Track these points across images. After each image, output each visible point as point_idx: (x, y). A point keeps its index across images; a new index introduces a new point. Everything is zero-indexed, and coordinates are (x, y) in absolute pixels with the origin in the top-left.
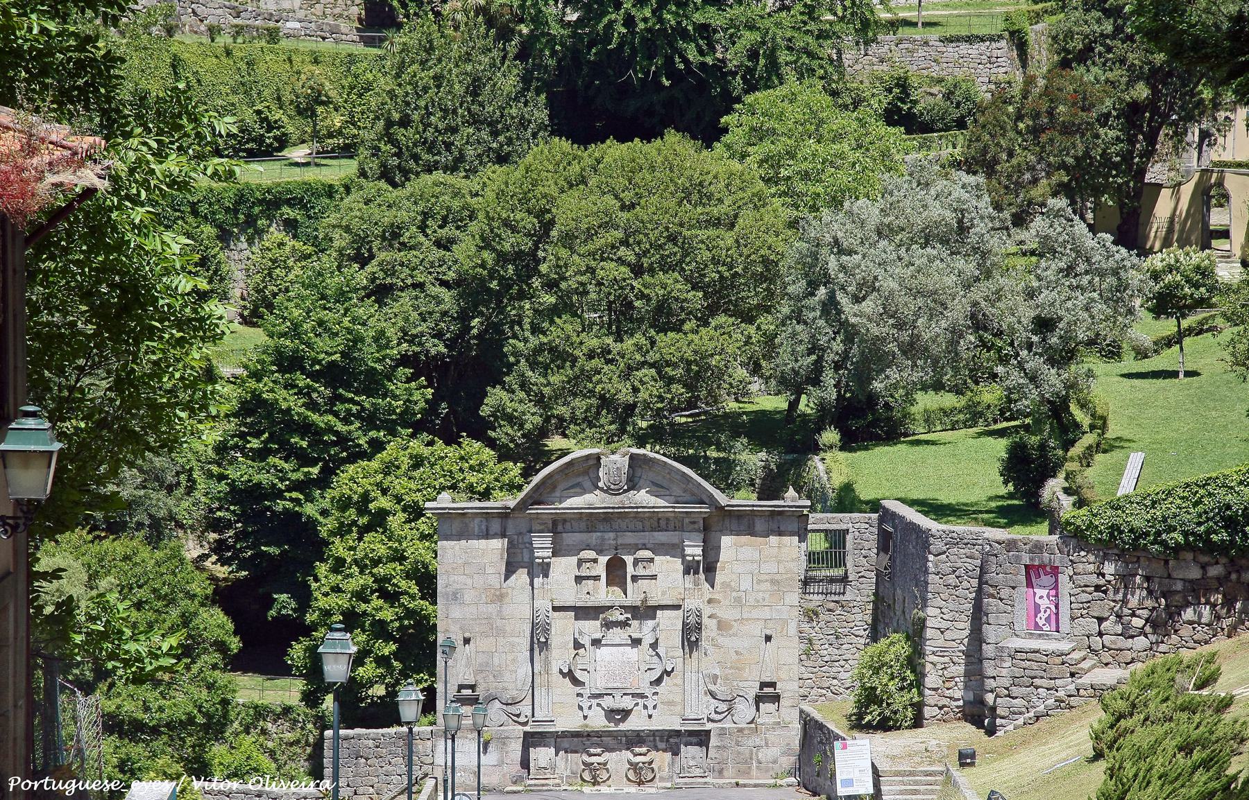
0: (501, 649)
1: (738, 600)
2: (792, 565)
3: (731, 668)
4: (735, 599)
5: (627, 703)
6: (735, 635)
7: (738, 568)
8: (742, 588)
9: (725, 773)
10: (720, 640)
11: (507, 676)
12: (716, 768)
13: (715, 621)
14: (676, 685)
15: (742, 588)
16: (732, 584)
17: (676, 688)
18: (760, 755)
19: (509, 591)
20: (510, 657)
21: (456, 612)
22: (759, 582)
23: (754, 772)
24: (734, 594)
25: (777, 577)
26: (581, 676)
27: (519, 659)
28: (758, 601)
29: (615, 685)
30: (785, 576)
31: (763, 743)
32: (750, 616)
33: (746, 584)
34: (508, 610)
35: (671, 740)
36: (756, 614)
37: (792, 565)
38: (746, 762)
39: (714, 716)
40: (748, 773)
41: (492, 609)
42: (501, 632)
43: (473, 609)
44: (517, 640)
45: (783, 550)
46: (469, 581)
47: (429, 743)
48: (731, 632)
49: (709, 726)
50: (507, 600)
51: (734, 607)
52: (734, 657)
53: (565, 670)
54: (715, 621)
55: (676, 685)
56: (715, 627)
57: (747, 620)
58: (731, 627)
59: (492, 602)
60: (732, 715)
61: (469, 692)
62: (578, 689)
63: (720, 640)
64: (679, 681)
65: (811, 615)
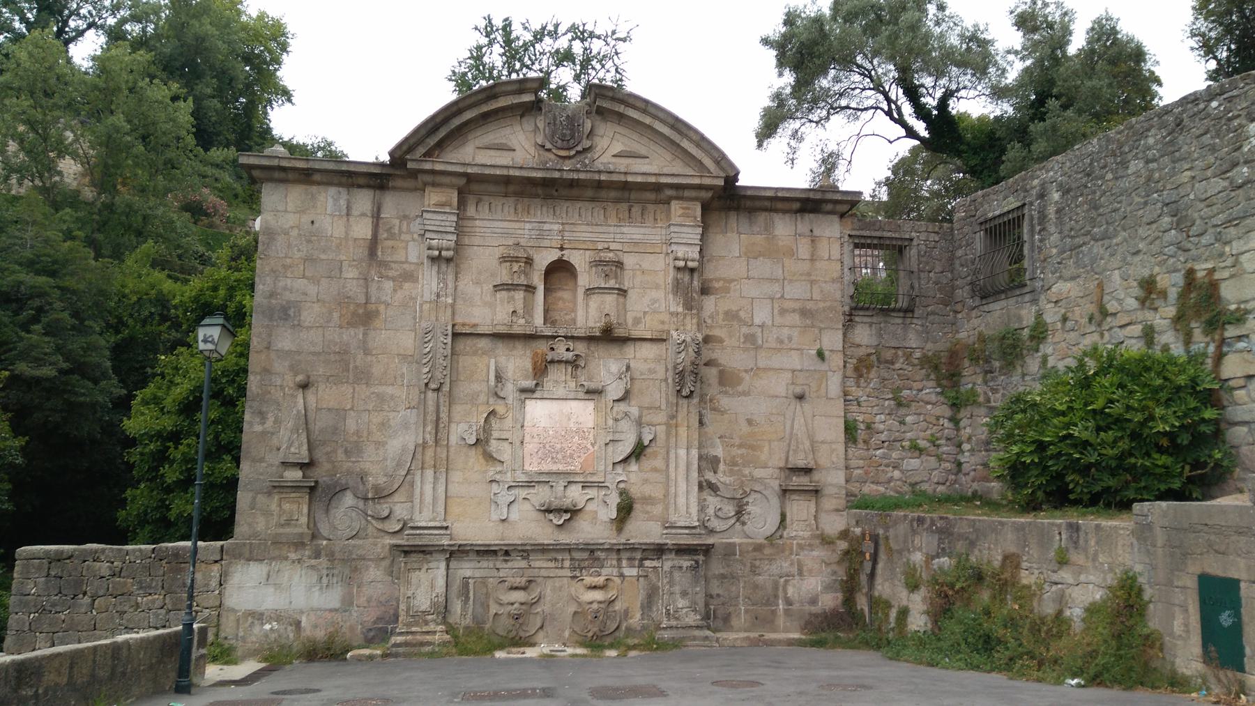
1: (750, 338)
2: (829, 288)
3: (740, 446)
5: (575, 495)
6: (746, 394)
7: (751, 290)
8: (757, 321)
9: (735, 622)
10: (724, 402)
11: (370, 453)
14: (655, 470)
15: (757, 321)
16: (742, 314)
17: (656, 475)
18: (790, 591)
19: (382, 308)
21: (285, 340)
22: (783, 312)
23: (781, 621)
24: (745, 330)
25: (810, 305)
26: (498, 451)
27: (392, 423)
28: (782, 342)
29: (554, 468)
30: (821, 305)
31: (795, 570)
33: (762, 315)
34: (380, 337)
35: (647, 563)
36: (777, 361)
37: (829, 288)
38: (768, 603)
40: (772, 622)
41: (352, 336)
42: (363, 376)
44: (389, 390)
45: (818, 264)
46: (312, 290)
47: (216, 567)
48: (740, 388)
50: (377, 323)
52: (745, 428)
55: (655, 470)
57: (766, 369)
58: (739, 381)
59: (351, 324)
60: (744, 524)
61: (297, 474)
62: (492, 472)
63: (724, 402)
65: (861, 368)
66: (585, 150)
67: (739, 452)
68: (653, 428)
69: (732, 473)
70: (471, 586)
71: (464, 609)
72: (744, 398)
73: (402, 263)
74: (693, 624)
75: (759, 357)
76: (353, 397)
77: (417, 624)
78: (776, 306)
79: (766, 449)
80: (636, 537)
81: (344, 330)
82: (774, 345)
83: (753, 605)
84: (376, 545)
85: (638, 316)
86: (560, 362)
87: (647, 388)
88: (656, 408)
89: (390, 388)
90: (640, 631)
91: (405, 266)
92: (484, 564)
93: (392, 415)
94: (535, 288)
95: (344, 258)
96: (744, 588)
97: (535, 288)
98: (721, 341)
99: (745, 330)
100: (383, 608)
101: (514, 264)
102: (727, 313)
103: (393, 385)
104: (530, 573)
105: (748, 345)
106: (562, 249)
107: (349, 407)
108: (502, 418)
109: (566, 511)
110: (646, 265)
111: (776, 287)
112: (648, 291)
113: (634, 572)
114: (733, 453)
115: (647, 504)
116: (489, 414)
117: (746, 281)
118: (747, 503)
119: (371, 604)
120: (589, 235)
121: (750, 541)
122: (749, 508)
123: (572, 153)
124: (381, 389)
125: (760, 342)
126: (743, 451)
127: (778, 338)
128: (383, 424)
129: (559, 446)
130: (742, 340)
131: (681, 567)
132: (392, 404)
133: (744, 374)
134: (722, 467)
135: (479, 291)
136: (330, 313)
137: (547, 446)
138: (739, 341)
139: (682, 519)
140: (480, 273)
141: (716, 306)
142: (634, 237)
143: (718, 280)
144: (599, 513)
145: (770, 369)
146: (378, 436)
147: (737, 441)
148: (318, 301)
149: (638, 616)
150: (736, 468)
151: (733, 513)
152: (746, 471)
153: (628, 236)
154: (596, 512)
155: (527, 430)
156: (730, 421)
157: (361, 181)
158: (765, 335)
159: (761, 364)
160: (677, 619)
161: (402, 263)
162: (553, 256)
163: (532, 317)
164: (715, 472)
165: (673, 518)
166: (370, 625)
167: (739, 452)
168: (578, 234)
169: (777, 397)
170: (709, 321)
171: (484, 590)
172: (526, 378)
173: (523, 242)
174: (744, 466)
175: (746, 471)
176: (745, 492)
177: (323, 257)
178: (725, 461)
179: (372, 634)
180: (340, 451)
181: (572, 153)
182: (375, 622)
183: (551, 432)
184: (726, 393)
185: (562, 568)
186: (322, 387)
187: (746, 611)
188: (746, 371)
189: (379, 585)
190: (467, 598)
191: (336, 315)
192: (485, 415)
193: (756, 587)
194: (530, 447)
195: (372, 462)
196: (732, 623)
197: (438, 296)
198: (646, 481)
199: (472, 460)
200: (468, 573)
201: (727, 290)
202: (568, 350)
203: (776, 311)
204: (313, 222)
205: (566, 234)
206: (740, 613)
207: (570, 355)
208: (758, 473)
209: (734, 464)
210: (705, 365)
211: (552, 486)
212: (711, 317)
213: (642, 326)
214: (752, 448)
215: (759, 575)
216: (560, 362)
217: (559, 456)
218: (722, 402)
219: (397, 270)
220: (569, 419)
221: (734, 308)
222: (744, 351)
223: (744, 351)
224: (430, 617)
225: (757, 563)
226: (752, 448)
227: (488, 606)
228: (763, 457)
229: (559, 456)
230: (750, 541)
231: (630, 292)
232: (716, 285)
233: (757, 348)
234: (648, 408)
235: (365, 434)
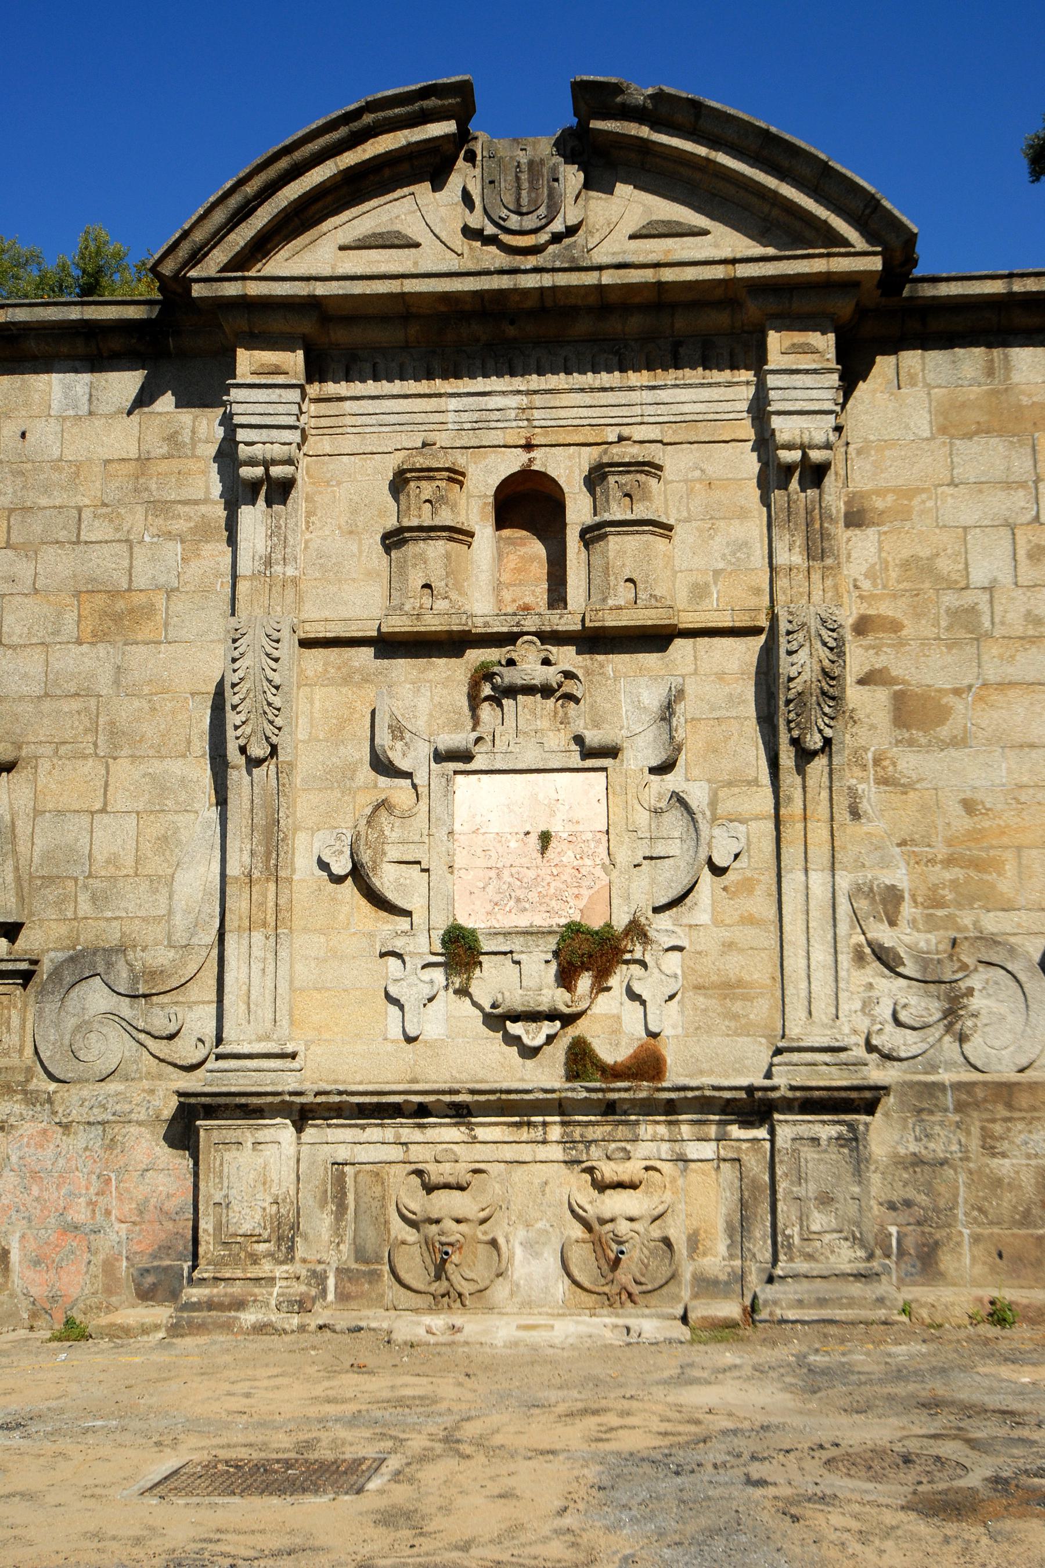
0: (119, 801)
3: (949, 862)
4: (954, 614)
6: (959, 742)
8: (979, 576)
9: (946, 1261)
12: (910, 1244)
13: (882, 695)
14: (749, 920)
15: (979, 576)
16: (944, 565)
17: (751, 932)
19: (160, 600)
20: (154, 828)
24: (950, 599)
26: (400, 887)
27: (184, 835)
32: (1013, 672)
39: (890, 1038)
43: (32, 663)
46: (24, 569)
48: (944, 732)
49: (877, 1074)
51: (953, 644)
52: (962, 822)
53: (341, 866)
54: (882, 695)
55: (749, 920)
56: (883, 718)
57: (1004, 686)
58: (943, 714)
59: (98, 637)
60: (962, 1038)
64: (763, 906)
66: (572, 231)
67: (948, 875)
68: (742, 828)
69: (931, 924)
70: (349, 1182)
71: (337, 1230)
72: (953, 752)
73: (196, 502)
74: (848, 1268)
75: (985, 658)
76: (106, 785)
77: (236, 1261)
78: (1021, 540)
79: (1010, 869)
80: (711, 1072)
81: (85, 648)
82: (1019, 631)
83: (991, 1223)
84: (152, 1092)
85: (701, 579)
86: (529, 690)
87: (727, 739)
88: (749, 783)
89: (180, 762)
90: (727, 1283)
91: (203, 509)
92: (374, 1133)
93: (182, 819)
94: (471, 535)
95: (87, 502)
96: (968, 1186)
97: (471, 535)
98: (895, 627)
99: (950, 599)
100: (169, 1225)
101: (424, 484)
102: (906, 565)
103: (184, 756)
104: (480, 1152)
105: (962, 634)
106: (529, 447)
107: (98, 806)
108: (406, 816)
109: (552, 1016)
110: (714, 470)
111: (1020, 498)
112: (722, 524)
113: (708, 1150)
114: (933, 879)
115: (734, 998)
116: (377, 808)
117: (950, 490)
118: (970, 991)
119: (147, 1217)
120: (585, 412)
121: (976, 1076)
122: (976, 1002)
123: (544, 237)
124: (157, 767)
125: (987, 624)
126: (956, 873)
127: (1029, 613)
128: (165, 839)
129: (531, 874)
130: (943, 624)
131: (815, 1141)
132: (183, 796)
133: (950, 700)
134: (907, 910)
135: (354, 548)
136: (59, 615)
137: (506, 875)
138: (937, 620)
139: (816, 1030)
140: (354, 512)
141: (880, 550)
142: (686, 408)
143: (880, 492)
144: (625, 1018)
145: (1011, 684)
146: (155, 865)
147: (941, 851)
148: (36, 591)
149: (722, 1247)
150: (940, 913)
151: (938, 1015)
152: (966, 919)
153: (675, 408)
154: (618, 1018)
155: (461, 839)
156: (924, 808)
157: (116, 344)
158: (998, 609)
159: (992, 673)
160: (810, 1257)
161: (196, 502)
162: (512, 462)
163: (462, 593)
164: (892, 923)
165: (797, 1029)
166: (145, 1263)
167: (948, 875)
168: (563, 413)
169: (1032, 746)
170: (866, 585)
171: (378, 1190)
172: (457, 727)
173: (442, 439)
174: (959, 906)
175: (966, 919)
176: (964, 967)
177: (43, 502)
178: (913, 897)
179: (150, 1279)
180: (83, 898)
181: (544, 237)
182: (154, 1256)
183: (513, 844)
184: (911, 743)
185: (544, 1142)
186: (44, 765)
187: (976, 1239)
188: (957, 692)
189: (161, 1178)
190: (341, 1208)
191: (70, 617)
192: (368, 811)
193: (997, 1183)
194: (467, 879)
195: (144, 919)
196: (942, 1267)
197: (268, 562)
198: (729, 946)
199: (346, 909)
200: (343, 1153)
201: (904, 514)
202: (546, 662)
203: (1021, 553)
204: (23, 435)
205: (537, 414)
206: (959, 1244)
207: (550, 675)
208: (993, 923)
209: (940, 904)
210: (861, 682)
211: (518, 963)
212: (870, 575)
213: (713, 601)
214: (976, 864)
215: (1004, 1155)
216: (529, 690)
217: (533, 896)
218: (902, 765)
219: (190, 519)
220: (553, 814)
221: (924, 552)
222: (950, 648)
223: (950, 648)
224: (262, 1247)
225: (998, 1128)
226: (976, 864)
227: (386, 1223)
228: (1005, 886)
229: (533, 896)
230: (976, 1076)
231: (679, 531)
232: (879, 503)
233: (979, 637)
234: (730, 784)
235: (129, 861)
